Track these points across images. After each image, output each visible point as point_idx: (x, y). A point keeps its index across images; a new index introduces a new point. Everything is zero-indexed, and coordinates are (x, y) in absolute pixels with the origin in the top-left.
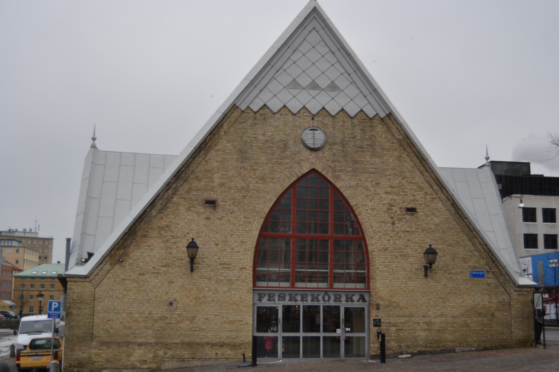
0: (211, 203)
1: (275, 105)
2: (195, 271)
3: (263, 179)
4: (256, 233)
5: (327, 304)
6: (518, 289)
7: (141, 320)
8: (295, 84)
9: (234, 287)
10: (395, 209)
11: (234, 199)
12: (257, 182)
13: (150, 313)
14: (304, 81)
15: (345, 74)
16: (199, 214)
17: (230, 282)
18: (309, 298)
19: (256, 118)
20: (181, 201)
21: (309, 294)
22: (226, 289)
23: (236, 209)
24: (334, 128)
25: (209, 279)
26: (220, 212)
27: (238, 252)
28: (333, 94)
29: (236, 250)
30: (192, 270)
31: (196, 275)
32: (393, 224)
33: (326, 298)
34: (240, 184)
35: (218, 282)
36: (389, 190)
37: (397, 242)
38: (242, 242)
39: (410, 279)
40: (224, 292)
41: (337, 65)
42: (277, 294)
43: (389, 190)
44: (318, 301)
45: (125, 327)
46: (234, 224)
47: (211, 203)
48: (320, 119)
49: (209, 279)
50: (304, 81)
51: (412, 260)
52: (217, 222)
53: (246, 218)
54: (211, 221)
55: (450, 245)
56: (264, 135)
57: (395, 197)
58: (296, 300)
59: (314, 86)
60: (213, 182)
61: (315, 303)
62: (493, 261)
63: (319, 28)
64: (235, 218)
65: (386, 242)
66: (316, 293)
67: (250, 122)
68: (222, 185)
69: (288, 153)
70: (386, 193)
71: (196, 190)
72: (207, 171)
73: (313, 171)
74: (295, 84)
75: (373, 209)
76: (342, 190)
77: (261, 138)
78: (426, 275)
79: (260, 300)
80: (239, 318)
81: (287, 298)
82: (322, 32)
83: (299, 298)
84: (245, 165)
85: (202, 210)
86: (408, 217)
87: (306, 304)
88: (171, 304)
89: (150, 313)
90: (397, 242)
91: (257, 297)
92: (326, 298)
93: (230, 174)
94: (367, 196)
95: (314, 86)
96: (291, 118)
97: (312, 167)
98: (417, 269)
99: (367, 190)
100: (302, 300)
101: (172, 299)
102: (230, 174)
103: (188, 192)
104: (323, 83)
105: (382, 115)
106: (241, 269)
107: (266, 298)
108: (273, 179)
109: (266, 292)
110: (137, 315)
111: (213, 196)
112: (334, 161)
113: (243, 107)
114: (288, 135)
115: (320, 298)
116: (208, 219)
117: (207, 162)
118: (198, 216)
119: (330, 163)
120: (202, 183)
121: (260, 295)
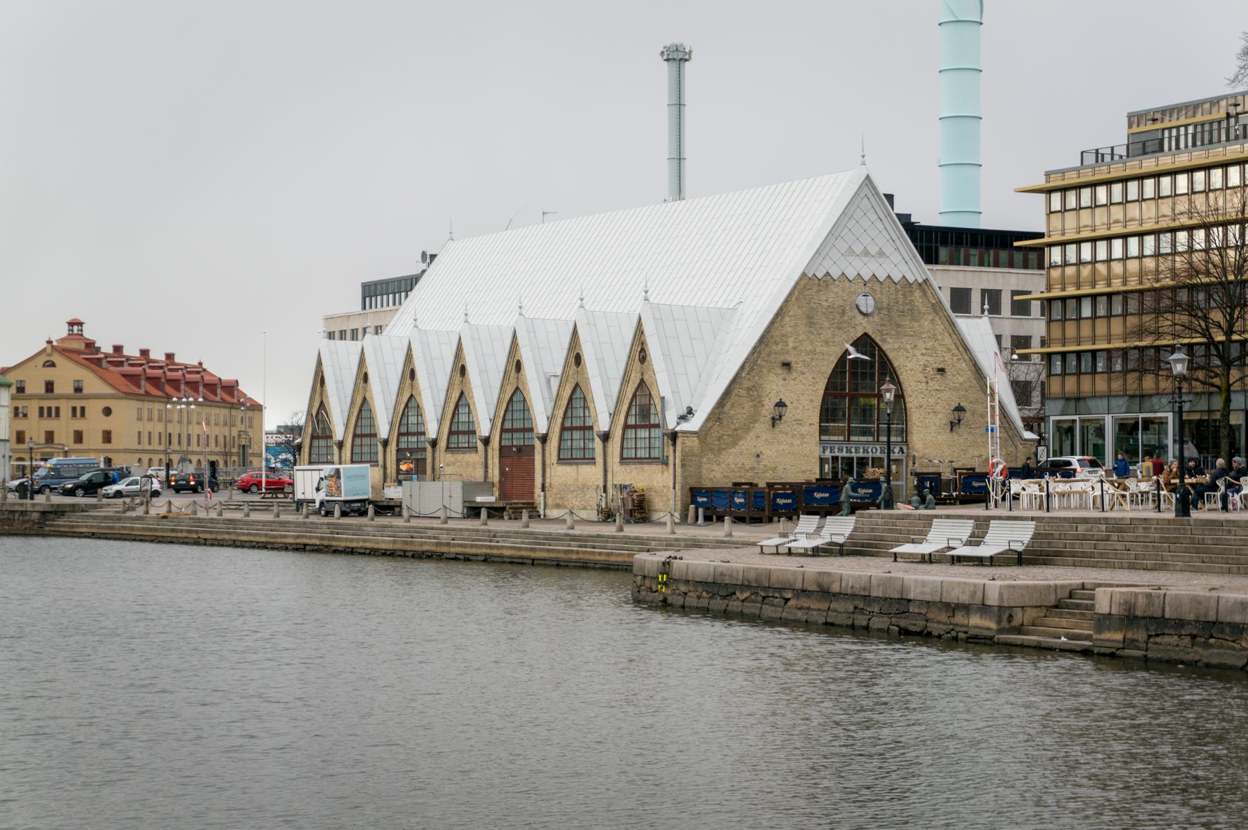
0: (787, 365)
1: (836, 274)
2: (776, 426)
3: (826, 342)
4: (821, 392)
5: (874, 455)
6: (1023, 442)
7: (736, 470)
8: (850, 251)
9: (805, 440)
10: (928, 369)
11: (804, 361)
12: (822, 346)
13: (743, 464)
14: (858, 249)
15: (891, 241)
16: (777, 375)
17: (802, 436)
18: (861, 450)
19: (819, 285)
20: (764, 363)
21: (861, 446)
22: (799, 442)
23: (806, 370)
24: (882, 293)
25: (786, 434)
26: (794, 374)
27: (808, 410)
28: (881, 261)
29: (806, 407)
30: (773, 426)
31: (777, 430)
32: (927, 383)
33: (874, 450)
34: (809, 348)
35: (793, 436)
36: (924, 351)
37: (930, 399)
38: (811, 401)
39: (939, 433)
40: (798, 446)
41: (884, 232)
42: (837, 446)
43: (924, 351)
44: (868, 452)
45: (725, 477)
46: (804, 384)
47: (787, 365)
48: (870, 285)
49: (786, 434)
50: (858, 249)
51: (940, 416)
52: (792, 382)
53: (814, 378)
54: (787, 381)
55: (971, 402)
56: (826, 301)
57: (929, 358)
58: (851, 452)
59: (866, 253)
60: (787, 345)
61: (866, 455)
62: (1005, 417)
63: (870, 195)
64: (806, 379)
65: (921, 400)
66: (867, 446)
67: (815, 289)
68: (795, 348)
69: (846, 318)
70: (922, 354)
71: (776, 353)
72: (783, 335)
73: (866, 334)
74: (850, 251)
75: (911, 370)
76: (887, 352)
77: (824, 303)
78: (952, 430)
79: (824, 452)
80: (809, 468)
81: (845, 450)
82: (872, 199)
83: (853, 450)
84: (813, 330)
85: (780, 372)
86: (938, 377)
87: (859, 455)
88: (758, 456)
89: (743, 464)
90: (930, 399)
91: (822, 449)
92: (874, 450)
93: (801, 338)
94: (907, 357)
95: (866, 253)
96: (847, 284)
97: (865, 331)
98: (945, 424)
99: (908, 352)
100: (856, 452)
101: (759, 452)
102: (801, 338)
103: (769, 355)
104: (873, 250)
105: (920, 281)
106: (810, 424)
107: (829, 450)
108: (834, 342)
109: (829, 445)
110: (733, 466)
111: (788, 359)
112: (881, 325)
113: (810, 275)
114: (845, 301)
115: (870, 450)
116: (785, 379)
117: (782, 327)
118: (777, 377)
119: (879, 328)
120: (780, 347)
121: (823, 447)
